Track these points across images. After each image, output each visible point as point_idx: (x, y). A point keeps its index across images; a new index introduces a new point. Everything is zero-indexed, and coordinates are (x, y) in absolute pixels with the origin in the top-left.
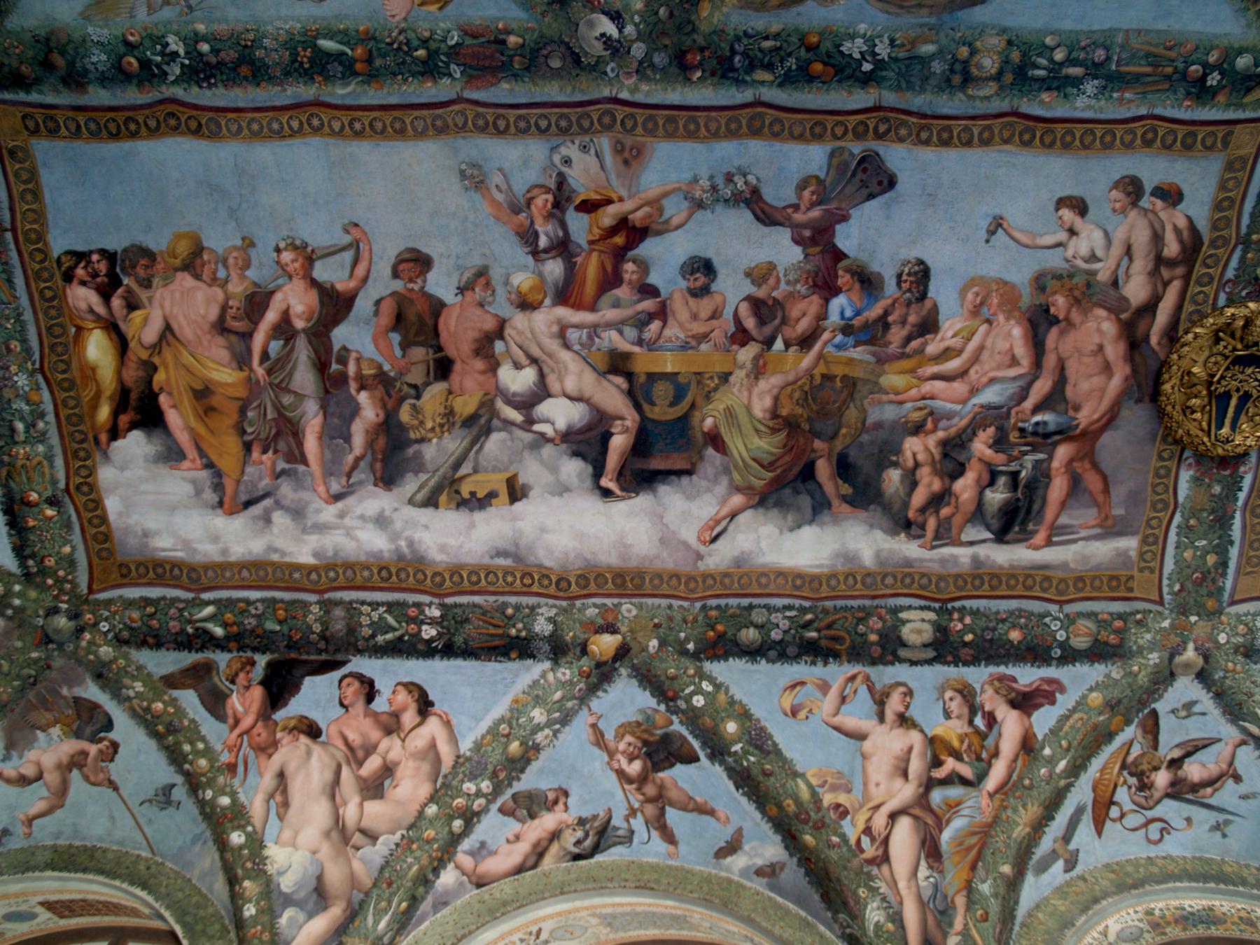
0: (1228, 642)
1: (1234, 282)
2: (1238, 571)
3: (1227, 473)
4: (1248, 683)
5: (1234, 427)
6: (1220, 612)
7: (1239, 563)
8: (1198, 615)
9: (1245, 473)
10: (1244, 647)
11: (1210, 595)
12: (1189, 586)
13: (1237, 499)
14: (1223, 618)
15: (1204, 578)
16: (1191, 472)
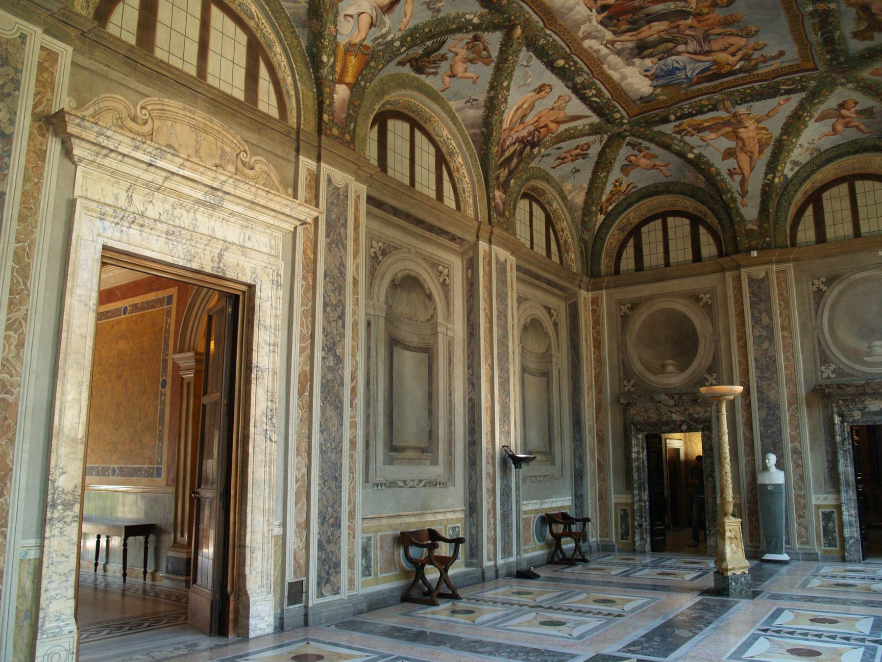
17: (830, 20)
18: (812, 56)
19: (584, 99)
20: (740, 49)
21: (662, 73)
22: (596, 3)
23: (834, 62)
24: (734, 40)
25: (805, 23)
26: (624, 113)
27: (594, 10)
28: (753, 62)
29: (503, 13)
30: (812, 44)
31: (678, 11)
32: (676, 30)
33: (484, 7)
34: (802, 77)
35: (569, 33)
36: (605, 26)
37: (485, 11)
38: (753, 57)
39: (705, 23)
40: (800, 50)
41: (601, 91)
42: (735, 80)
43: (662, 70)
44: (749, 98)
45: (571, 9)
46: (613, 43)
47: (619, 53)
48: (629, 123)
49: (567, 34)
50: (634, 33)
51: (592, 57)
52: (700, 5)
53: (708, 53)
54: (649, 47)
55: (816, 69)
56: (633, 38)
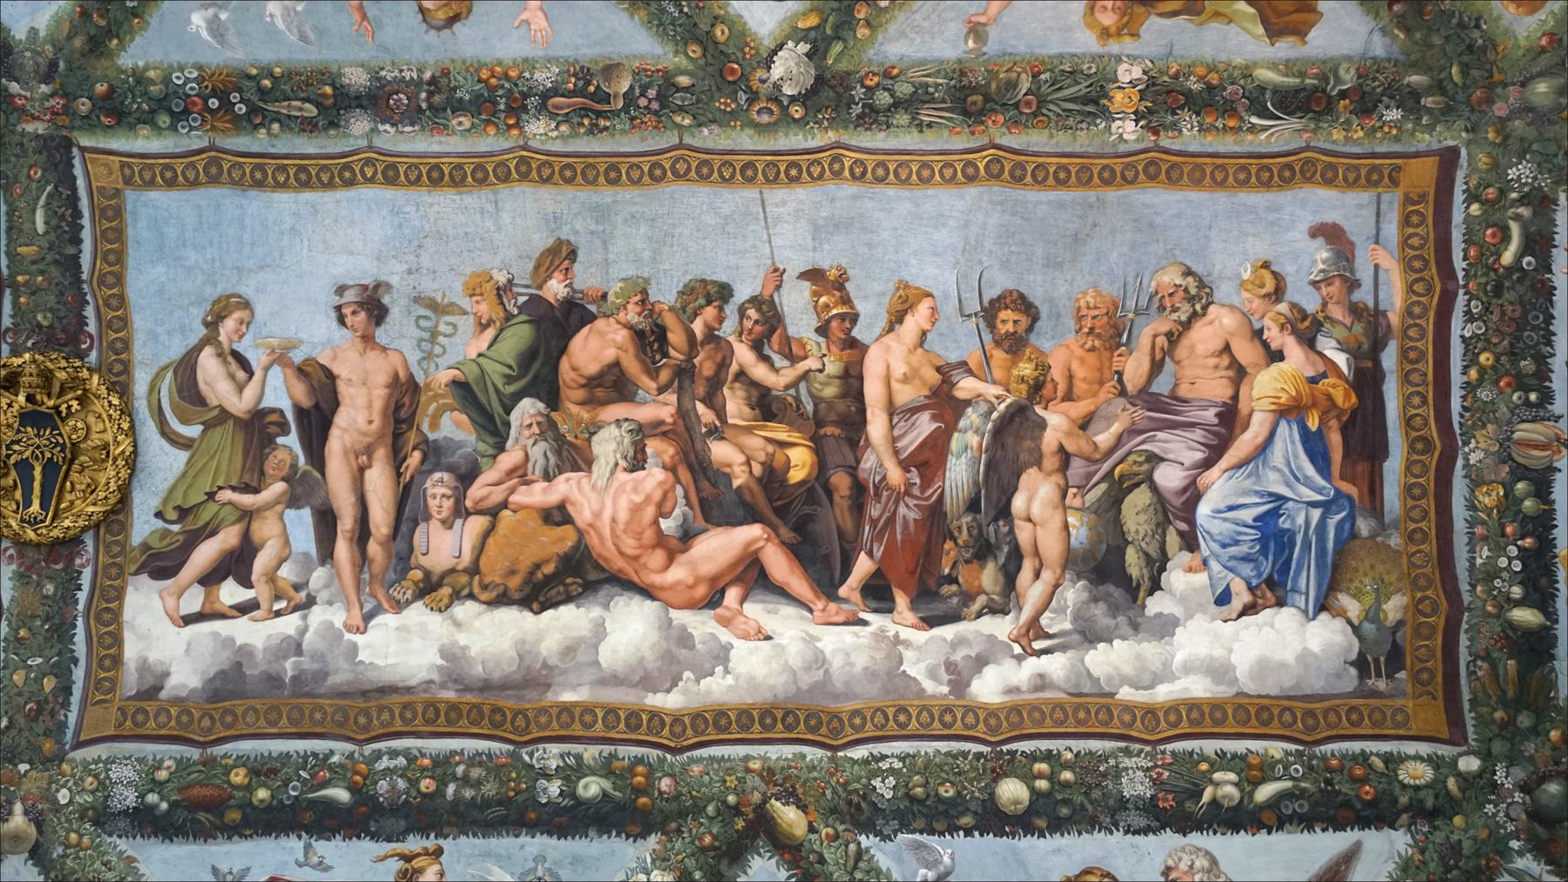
0: (71, 802)
1: (15, 329)
2: (84, 699)
3: (59, 566)
4: (97, 865)
5: (44, 506)
6: (60, 758)
7: (86, 688)
8: (30, 762)
9: (83, 566)
10: (94, 808)
11: (47, 733)
12: (21, 721)
13: (76, 602)
14: (65, 766)
15: (40, 711)
16: (14, 567)
17: (1194, 85)
18: (1374, 155)
19: (1238, 819)
20: (1258, 334)
21: (1267, 567)
22: (845, 601)
23: (1428, 101)
24: (1204, 337)
25: (1192, 148)
26: (1424, 748)
27: (863, 615)
28: (1337, 312)
29: (698, 809)
30: (1308, 148)
31: (999, 432)
32: (1077, 468)
33: (644, 835)
34: (1472, 197)
35: (902, 709)
36: (953, 618)
37: (653, 841)
38: (1311, 304)
39: (1080, 387)
40: (1328, 182)
41: (1243, 758)
42: (1405, 378)
43: (1246, 559)
44: (1527, 365)
45: (819, 660)
46: (1033, 629)
47: (1089, 636)
48: (1487, 757)
49: (898, 714)
50: (1028, 566)
51: (1058, 706)
52: (998, 373)
53: (1230, 419)
54: (1118, 550)
55: (1448, 159)
56: (1047, 575)
